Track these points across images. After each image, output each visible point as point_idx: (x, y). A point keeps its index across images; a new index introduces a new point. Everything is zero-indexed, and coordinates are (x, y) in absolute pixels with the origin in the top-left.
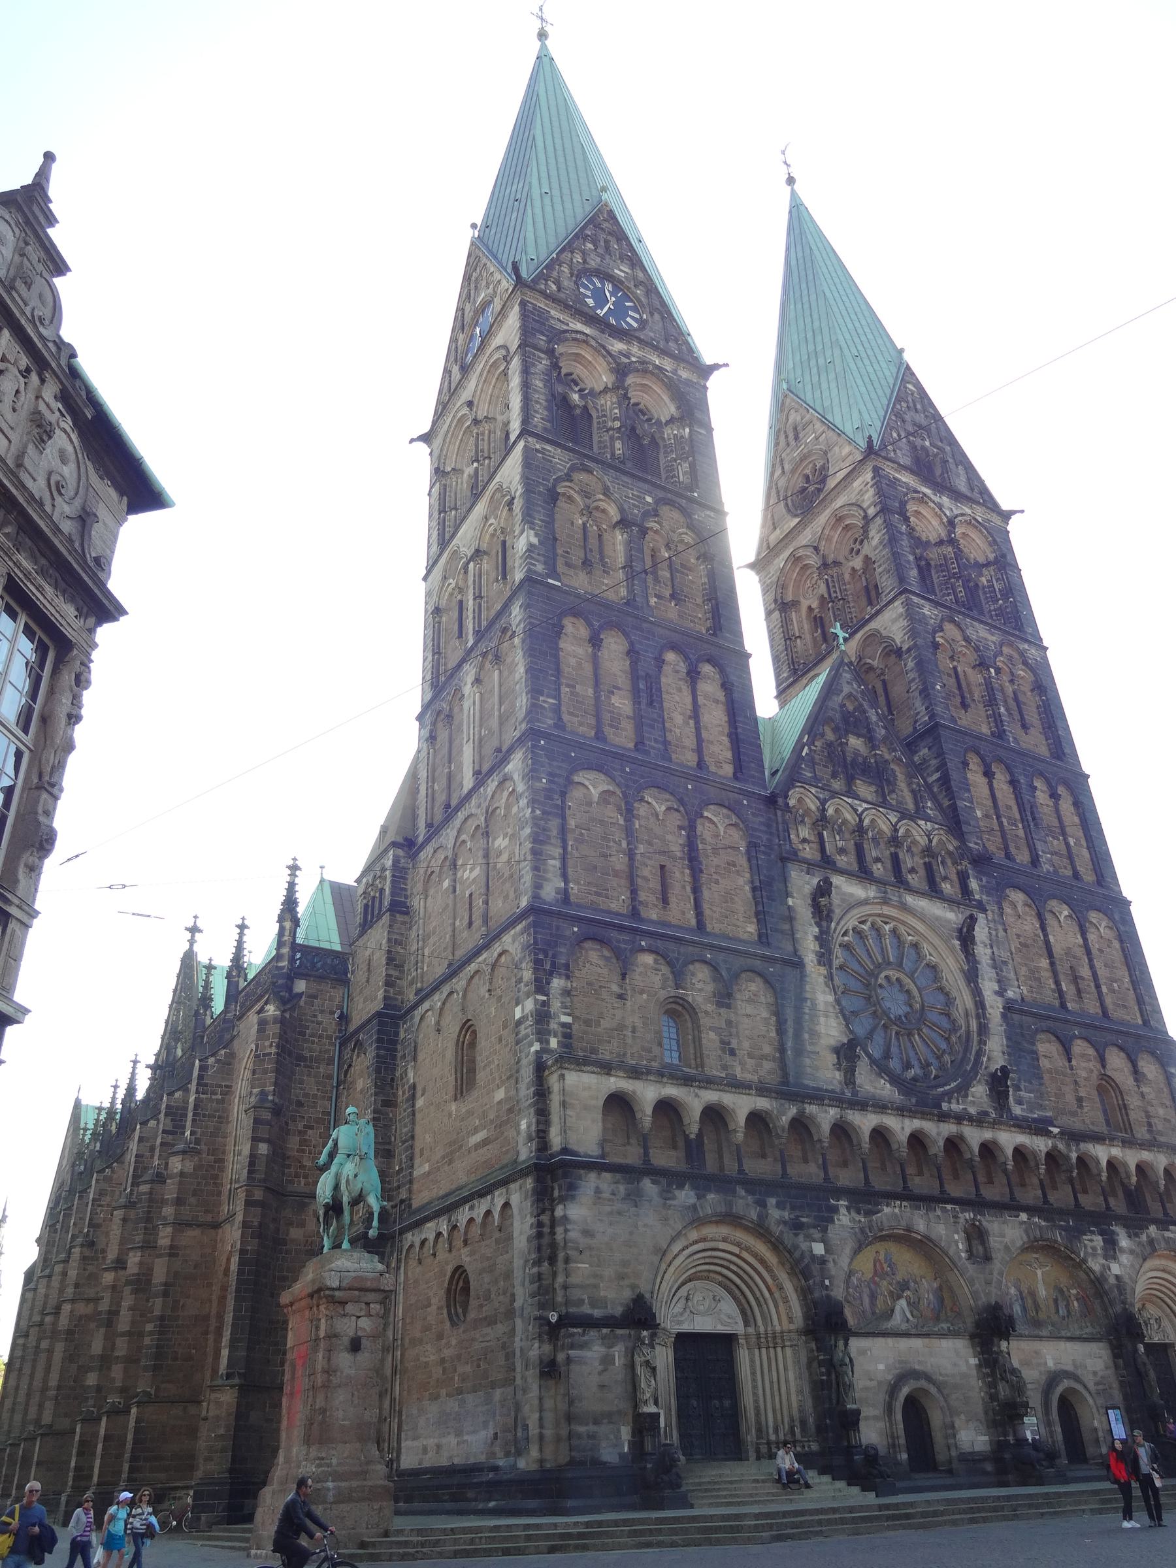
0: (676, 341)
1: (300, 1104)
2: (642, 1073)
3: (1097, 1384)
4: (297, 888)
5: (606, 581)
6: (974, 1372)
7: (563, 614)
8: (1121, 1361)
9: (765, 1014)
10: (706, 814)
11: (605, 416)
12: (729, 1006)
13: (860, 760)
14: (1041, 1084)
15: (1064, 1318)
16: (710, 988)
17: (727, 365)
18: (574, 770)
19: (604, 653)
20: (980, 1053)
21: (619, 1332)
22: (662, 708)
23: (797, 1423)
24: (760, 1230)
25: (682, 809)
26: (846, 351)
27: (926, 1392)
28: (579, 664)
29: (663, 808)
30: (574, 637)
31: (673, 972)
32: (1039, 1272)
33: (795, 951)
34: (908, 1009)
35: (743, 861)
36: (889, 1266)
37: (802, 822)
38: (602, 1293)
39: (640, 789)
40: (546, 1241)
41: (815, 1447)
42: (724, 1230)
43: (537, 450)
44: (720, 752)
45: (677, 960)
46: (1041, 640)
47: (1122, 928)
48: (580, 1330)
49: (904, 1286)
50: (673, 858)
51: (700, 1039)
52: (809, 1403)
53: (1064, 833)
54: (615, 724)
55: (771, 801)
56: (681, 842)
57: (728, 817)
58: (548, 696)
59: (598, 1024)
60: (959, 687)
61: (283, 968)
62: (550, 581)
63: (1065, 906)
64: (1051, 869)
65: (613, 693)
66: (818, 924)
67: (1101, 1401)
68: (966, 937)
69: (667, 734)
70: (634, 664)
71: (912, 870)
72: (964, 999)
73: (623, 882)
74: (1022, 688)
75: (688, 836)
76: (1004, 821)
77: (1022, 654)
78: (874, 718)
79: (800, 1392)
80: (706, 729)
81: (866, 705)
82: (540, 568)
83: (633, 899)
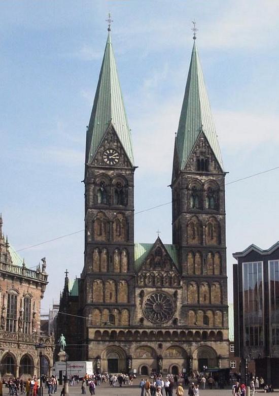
26: (186, 130)
33: (135, 303)
39: (108, 279)
46: (225, 211)
53: (214, 264)
54: (104, 268)
68: (176, 294)
72: (173, 305)
76: (196, 265)
77: (216, 218)
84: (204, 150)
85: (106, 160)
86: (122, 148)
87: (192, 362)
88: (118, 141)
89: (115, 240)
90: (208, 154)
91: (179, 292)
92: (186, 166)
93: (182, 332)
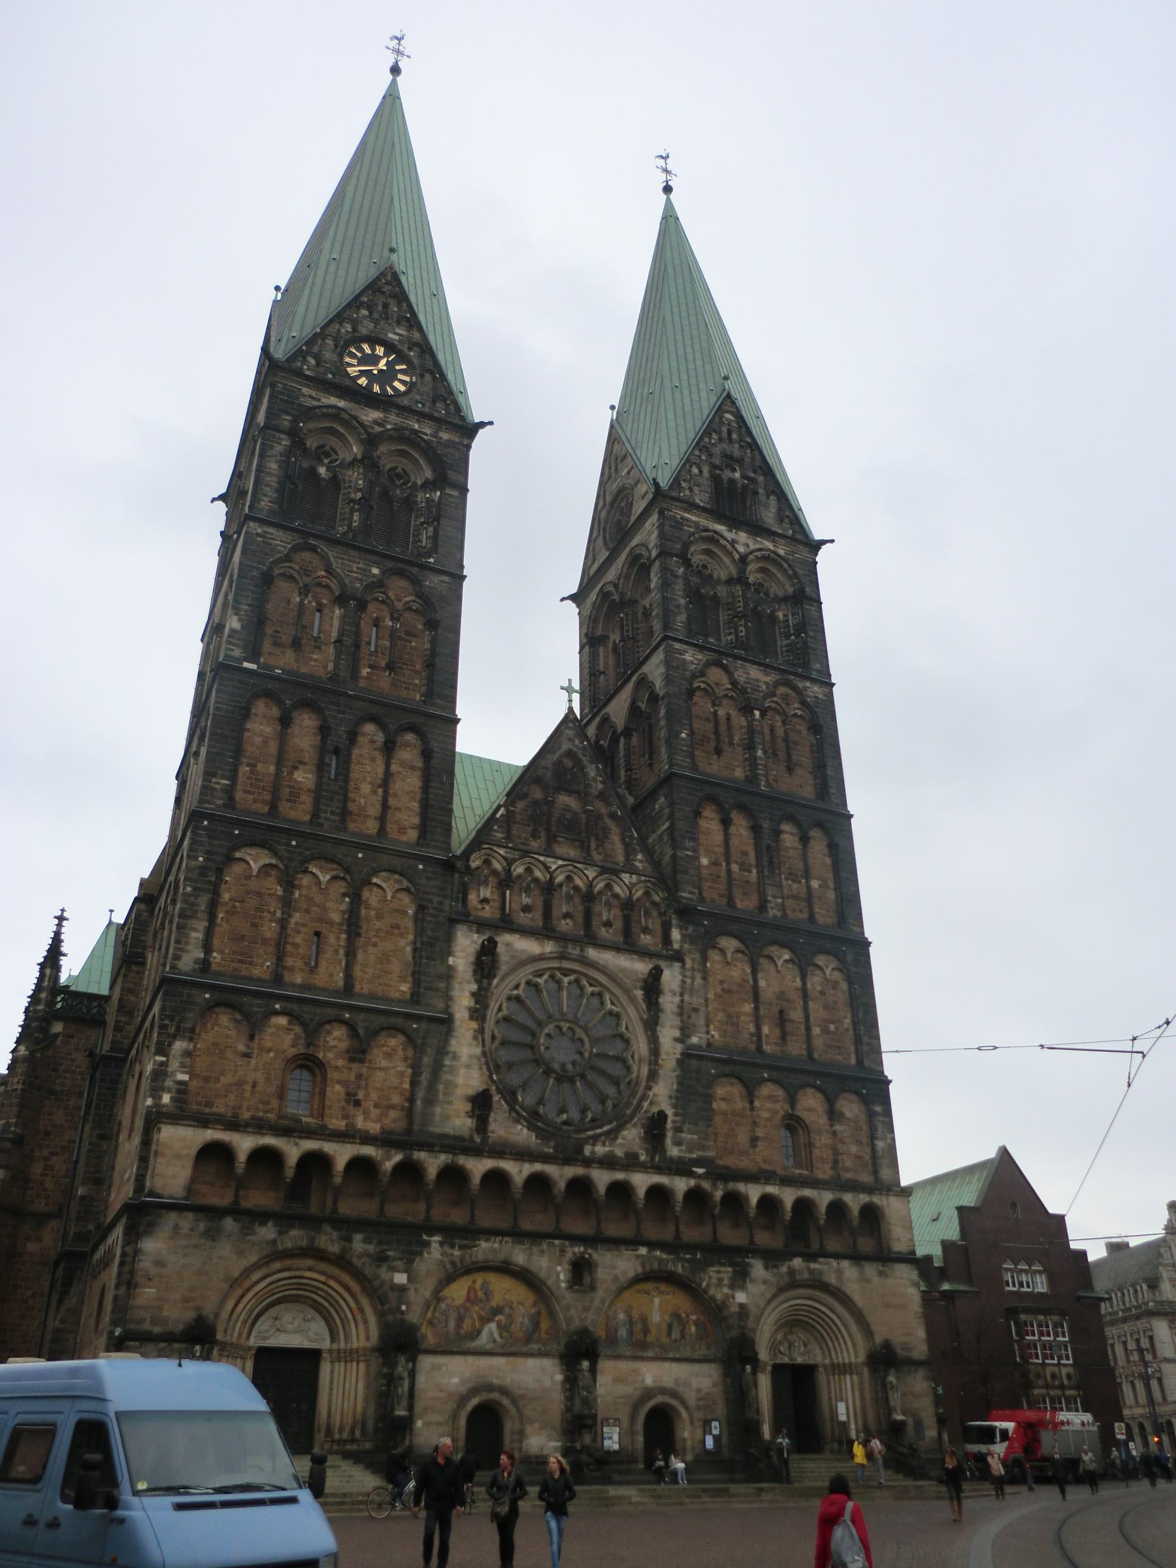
0: (445, 400)
1: (47, 1134)
2: (240, 1126)
3: (698, 1399)
4: (63, 937)
5: (315, 657)
6: (559, 1387)
7: (256, 696)
8: (728, 1380)
9: (401, 1067)
10: (375, 880)
11: (350, 487)
12: (362, 1061)
13: (569, 816)
14: (709, 1126)
15: (675, 1341)
16: (343, 1045)
17: (491, 423)
18: (237, 848)
19: (295, 729)
20: (644, 1097)
21: (176, 1346)
22: (347, 780)
23: (359, 1426)
24: (342, 1261)
25: (348, 877)
26: (667, 382)
27: (499, 1403)
28: (265, 742)
29: (328, 877)
30: (265, 717)
31: (305, 1032)
32: (657, 1300)
33: (448, 1007)
34: (577, 1057)
35: (411, 925)
36: (485, 1294)
37: (486, 883)
38: (165, 1314)
39: (307, 861)
40: (127, 1268)
41: (368, 1445)
42: (310, 1262)
43: (258, 535)
44: (407, 816)
45: (312, 1020)
46: (829, 676)
47: (853, 969)
48: (137, 1344)
49: (498, 1311)
50: (331, 923)
51: (325, 1090)
52: (371, 1410)
53: (807, 874)
54: (294, 798)
55: (449, 866)
56: (343, 907)
57: (399, 882)
58: (223, 777)
59: (217, 1080)
60: (717, 733)
61: (40, 1011)
62: (246, 665)
63: (786, 951)
64: (779, 914)
65: (296, 768)
66: (476, 981)
67: (699, 1415)
68: (652, 986)
69: (349, 804)
70: (324, 738)
71: (608, 924)
72: (641, 1046)
73: (271, 949)
74: (798, 727)
75: (351, 903)
76: (735, 867)
77: (800, 693)
78: (592, 774)
79: (366, 1400)
80: (395, 795)
81: (585, 760)
82: (237, 653)
83: (277, 966)
84: (736, 451)
85: (353, 371)
86: (426, 349)
87: (756, 1384)
88: (413, 322)
89: (362, 684)
90: (755, 472)
91: (671, 977)
92: (676, 482)
93: (695, 1197)
